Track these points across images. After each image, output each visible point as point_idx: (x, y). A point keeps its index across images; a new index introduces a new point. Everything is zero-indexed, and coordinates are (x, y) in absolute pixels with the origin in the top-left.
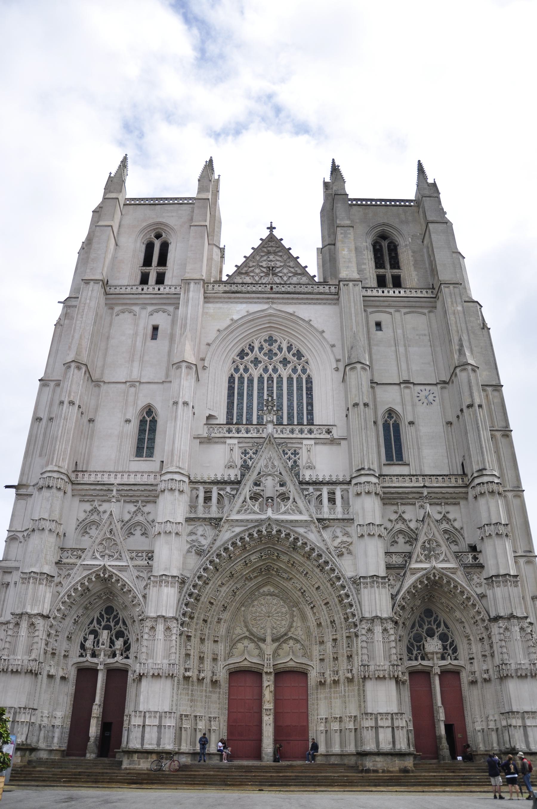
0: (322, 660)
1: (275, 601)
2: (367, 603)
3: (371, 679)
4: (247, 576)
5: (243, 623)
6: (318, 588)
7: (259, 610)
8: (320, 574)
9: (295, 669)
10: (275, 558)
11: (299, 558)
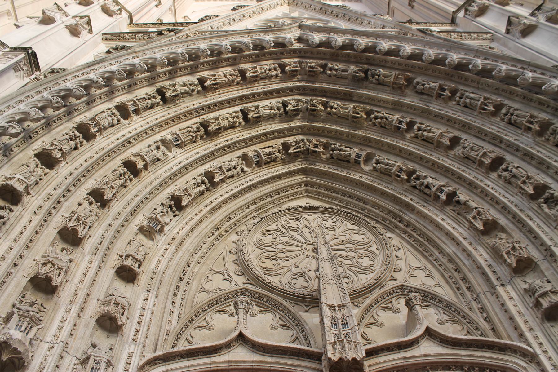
1: (329, 223)
5: (232, 268)
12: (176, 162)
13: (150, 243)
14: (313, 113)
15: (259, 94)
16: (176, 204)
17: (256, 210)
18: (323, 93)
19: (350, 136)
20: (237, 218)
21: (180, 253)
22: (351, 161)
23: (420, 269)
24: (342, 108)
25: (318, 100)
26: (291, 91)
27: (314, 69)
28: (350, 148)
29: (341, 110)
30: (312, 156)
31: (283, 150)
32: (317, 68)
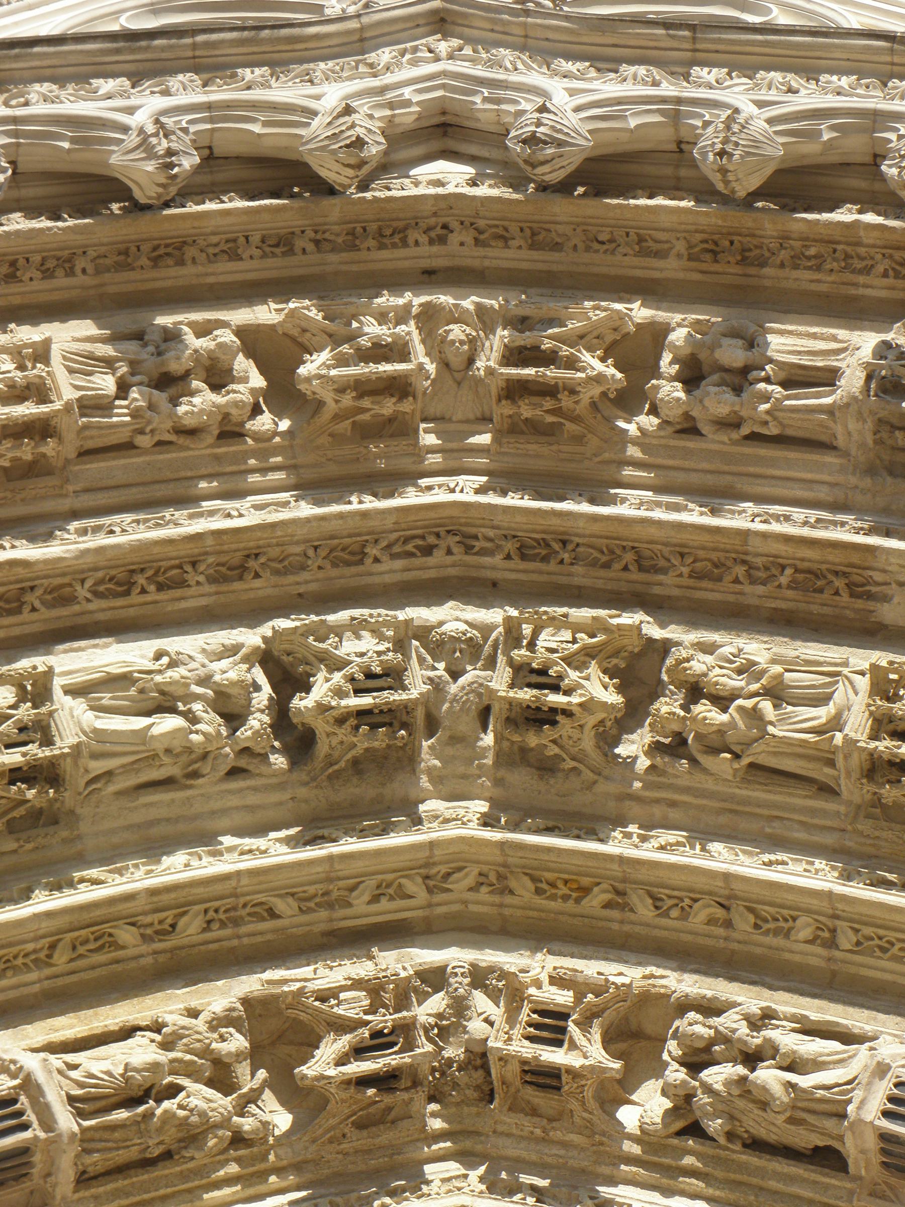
14: (532, 740)
18: (634, 571)
19: (846, 940)
22: (849, 1148)
24: (777, 693)
25: (576, 628)
27: (551, 373)
28: (847, 1038)
29: (766, 706)
30: (511, 1121)
31: (256, 1055)
32: (572, 364)
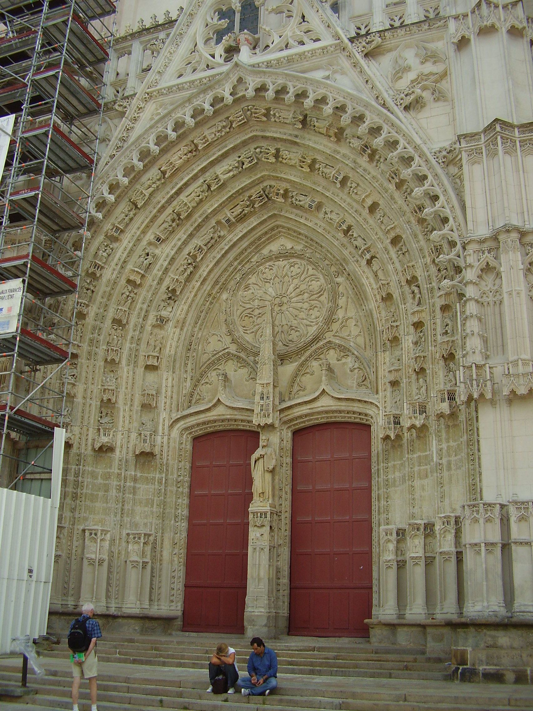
0: (394, 384)
1: (295, 270)
2: (480, 202)
3: (492, 402)
4: (220, 217)
5: (224, 329)
6: (373, 208)
7: (260, 293)
8: (370, 167)
9: (339, 418)
10: (273, 160)
11: (321, 145)
12: (165, 255)
13: (163, 332)
15: (216, 159)
16: (172, 296)
17: (239, 264)
20: (224, 279)
21: (185, 329)
23: (352, 318)
26: (245, 143)
